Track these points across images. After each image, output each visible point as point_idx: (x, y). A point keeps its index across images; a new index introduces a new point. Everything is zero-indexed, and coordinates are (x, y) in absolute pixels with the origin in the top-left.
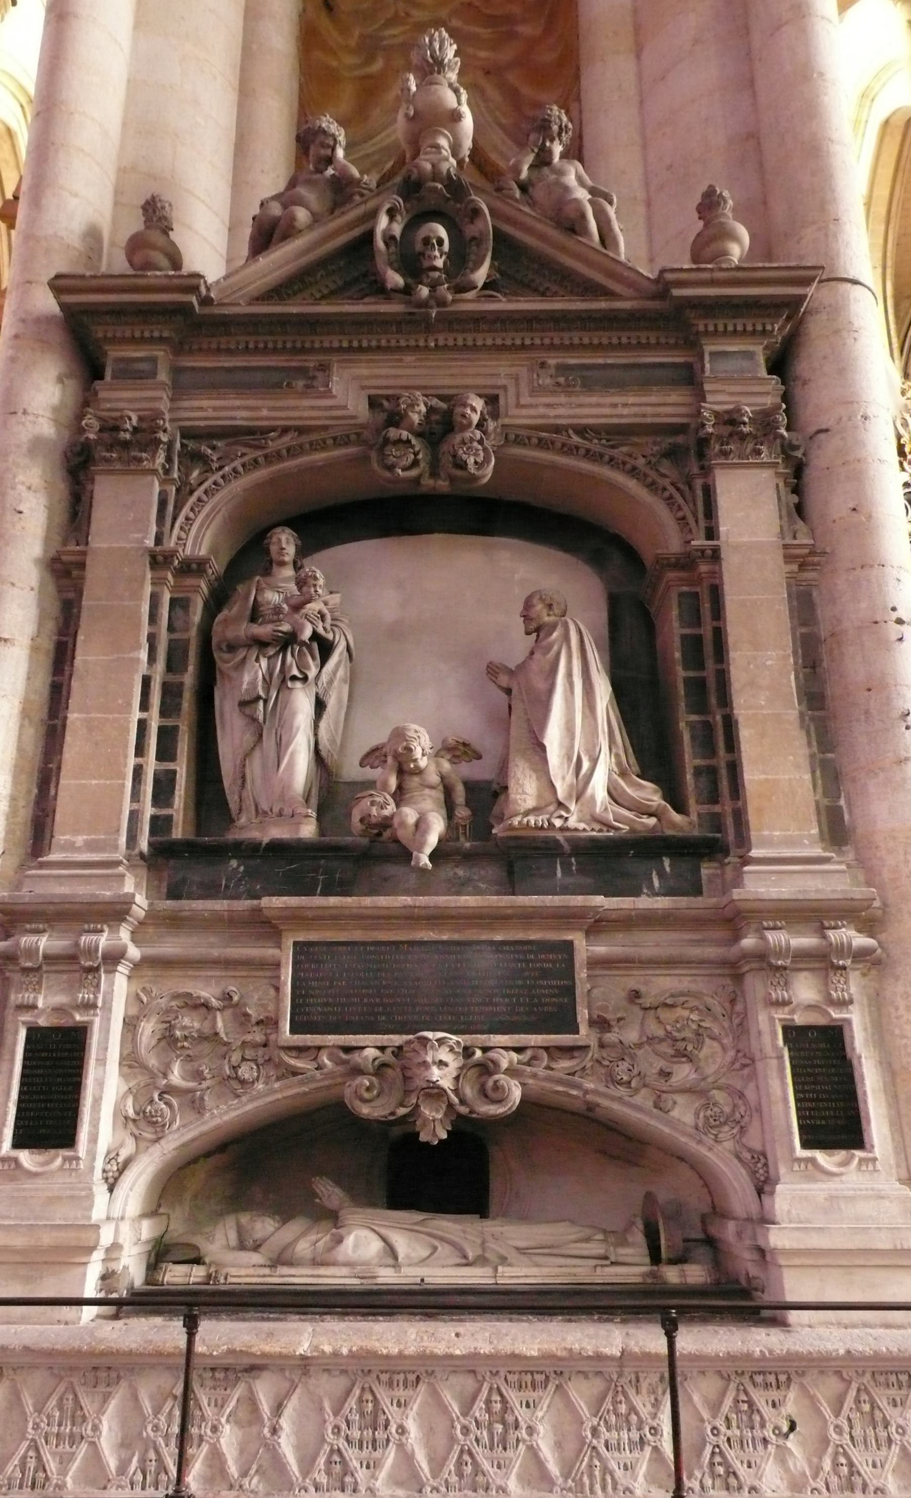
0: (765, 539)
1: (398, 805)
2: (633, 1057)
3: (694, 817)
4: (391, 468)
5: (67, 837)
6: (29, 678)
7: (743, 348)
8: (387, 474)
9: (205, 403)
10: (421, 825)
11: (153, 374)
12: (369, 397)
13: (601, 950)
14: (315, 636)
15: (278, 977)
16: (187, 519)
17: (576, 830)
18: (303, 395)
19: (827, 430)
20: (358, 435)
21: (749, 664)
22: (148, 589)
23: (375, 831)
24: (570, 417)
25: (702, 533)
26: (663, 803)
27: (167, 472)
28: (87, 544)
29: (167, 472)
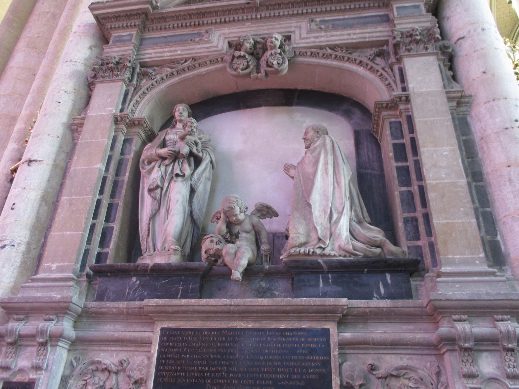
0: (435, 89)
5: (48, 264)
6: (49, 181)
12: (229, 42)
13: (347, 335)
15: (150, 352)
17: (329, 255)
19: (463, 38)
23: (213, 259)
24: (327, 41)
25: (400, 90)
26: (384, 239)
27: (131, 81)
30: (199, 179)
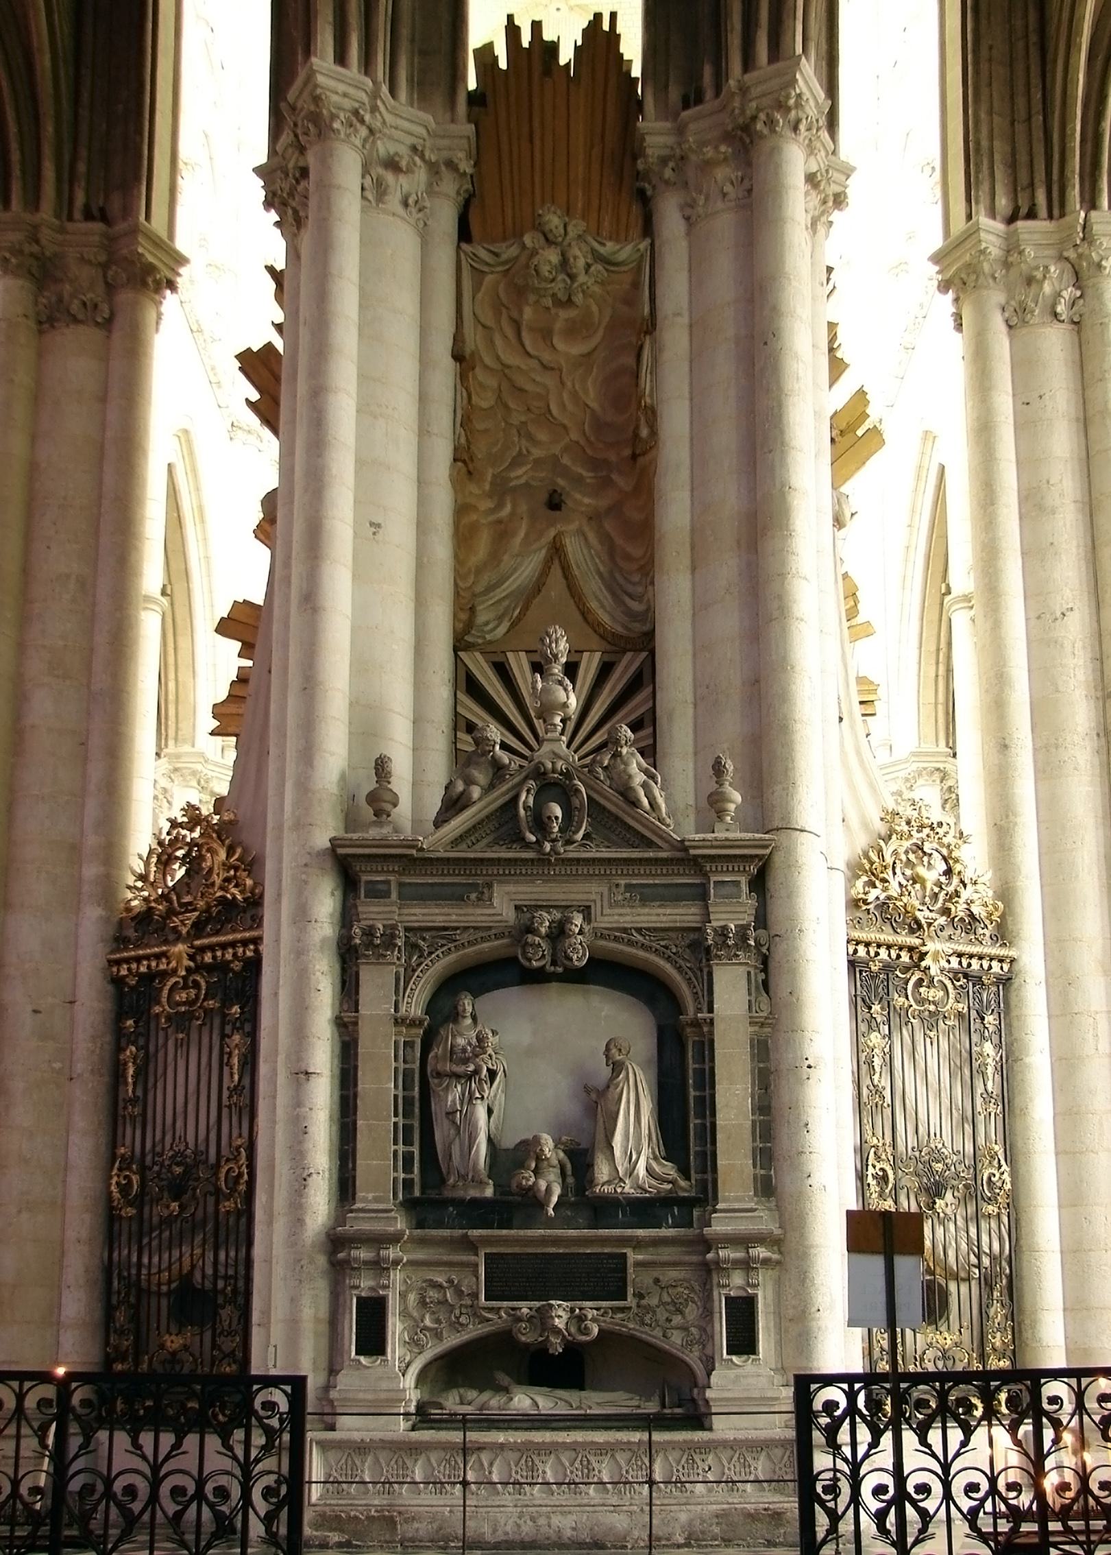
2: (654, 1312)
4: (530, 960)
9: (417, 911)
10: (549, 1190)
11: (387, 894)
13: (640, 1257)
26: (676, 1175)
28: (357, 1011)
29: (398, 959)
30: (495, 1096)
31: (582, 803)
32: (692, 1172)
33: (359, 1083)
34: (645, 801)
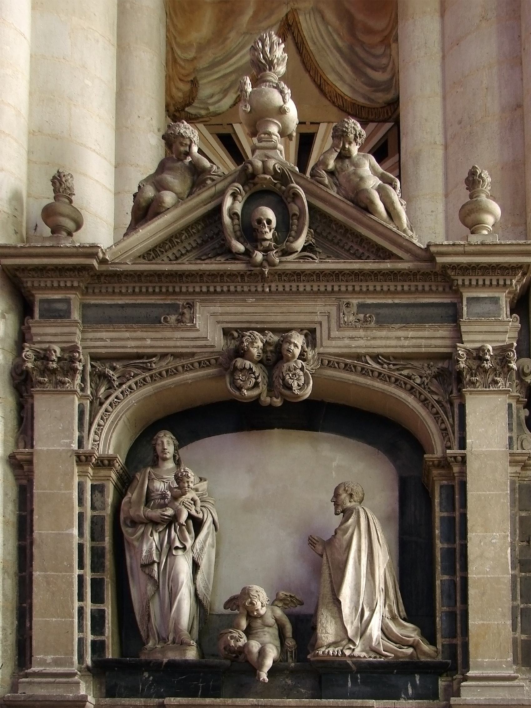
1: (248, 639)
3: (439, 647)
4: (239, 389)
5: (41, 656)
6: (4, 545)
7: (491, 295)
8: (237, 393)
10: (262, 653)
14: (190, 516)
16: (99, 425)
18: (176, 329)
20: (216, 359)
21: (481, 542)
22: (76, 480)
23: (234, 655)
24: (366, 347)
26: (418, 638)
27: (83, 390)
28: (32, 447)
29: (83, 390)
31: (302, 210)
32: (439, 636)
33: (35, 528)
34: (381, 207)
